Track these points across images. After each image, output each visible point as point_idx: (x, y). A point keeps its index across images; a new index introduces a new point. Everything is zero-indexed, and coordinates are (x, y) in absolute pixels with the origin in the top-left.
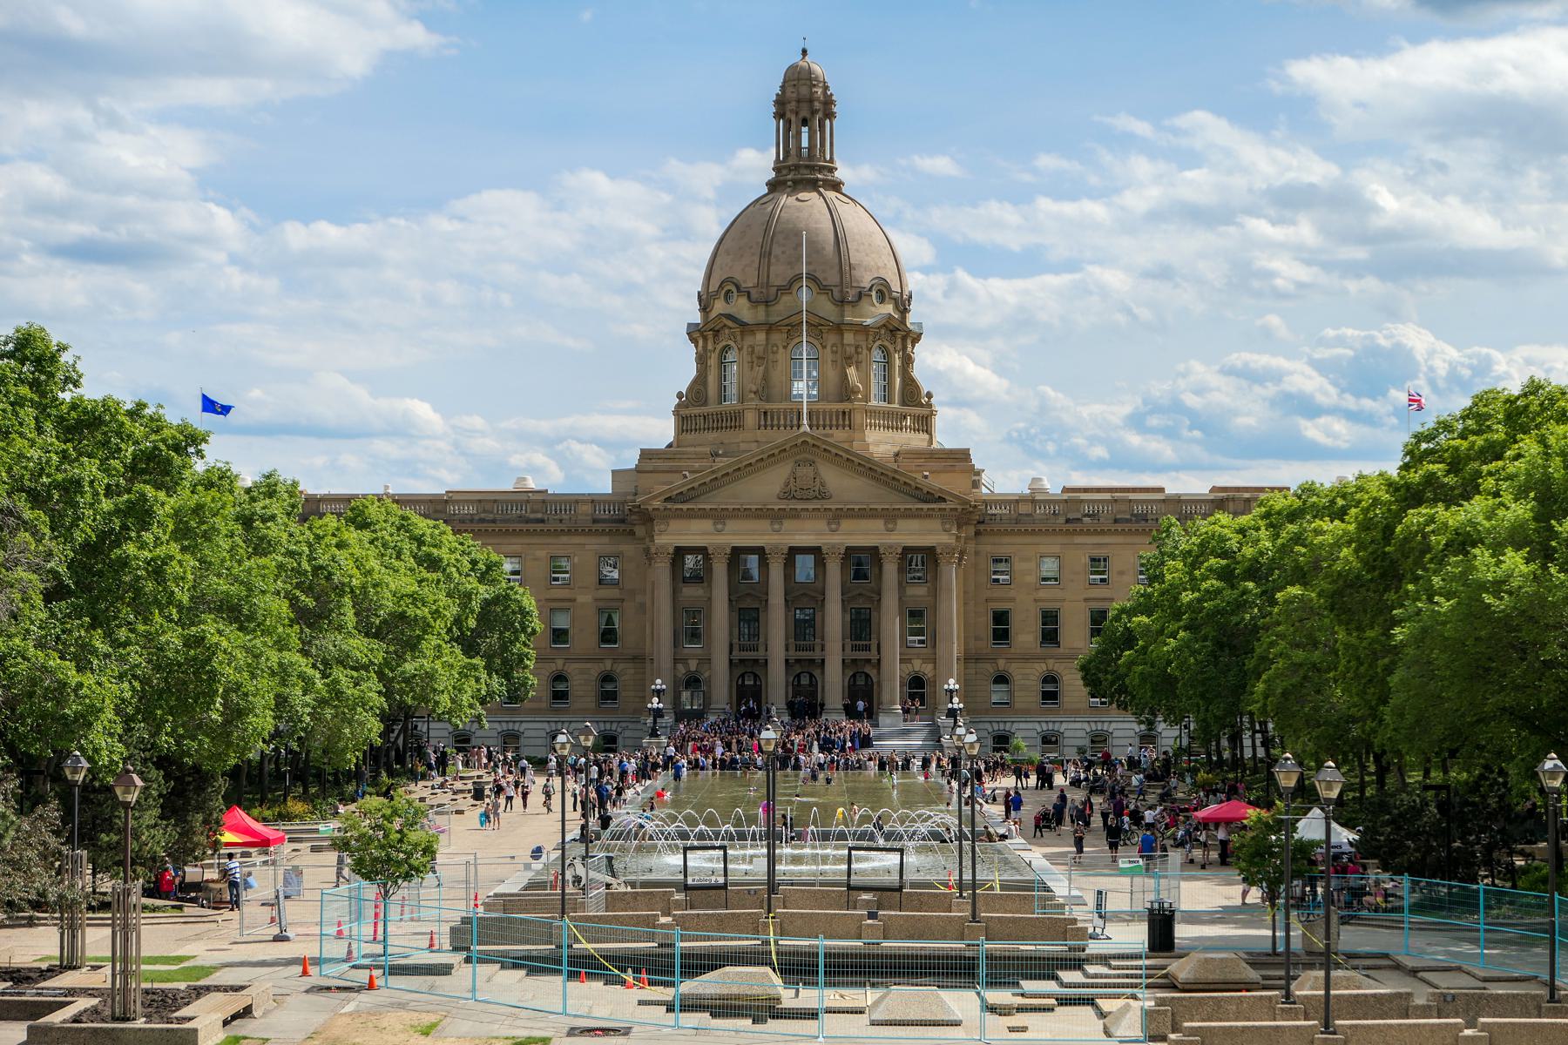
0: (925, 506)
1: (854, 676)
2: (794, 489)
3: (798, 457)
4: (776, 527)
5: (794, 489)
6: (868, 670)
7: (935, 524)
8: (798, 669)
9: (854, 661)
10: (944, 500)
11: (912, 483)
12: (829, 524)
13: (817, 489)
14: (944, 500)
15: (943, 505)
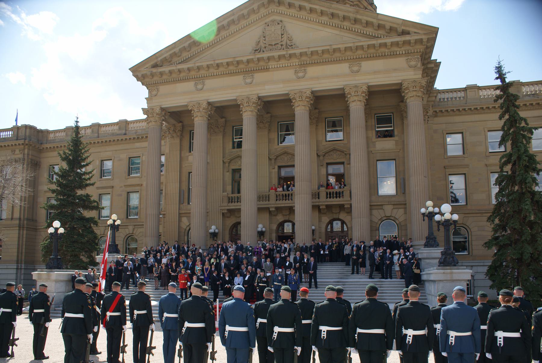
0: (389, 41)
1: (331, 223)
2: (263, 46)
3: (267, 20)
4: (249, 80)
5: (263, 46)
6: (342, 216)
7: (400, 62)
8: (280, 218)
9: (329, 207)
10: (408, 33)
11: (374, 21)
12: (296, 72)
13: (284, 43)
14: (408, 33)
15: (407, 38)
